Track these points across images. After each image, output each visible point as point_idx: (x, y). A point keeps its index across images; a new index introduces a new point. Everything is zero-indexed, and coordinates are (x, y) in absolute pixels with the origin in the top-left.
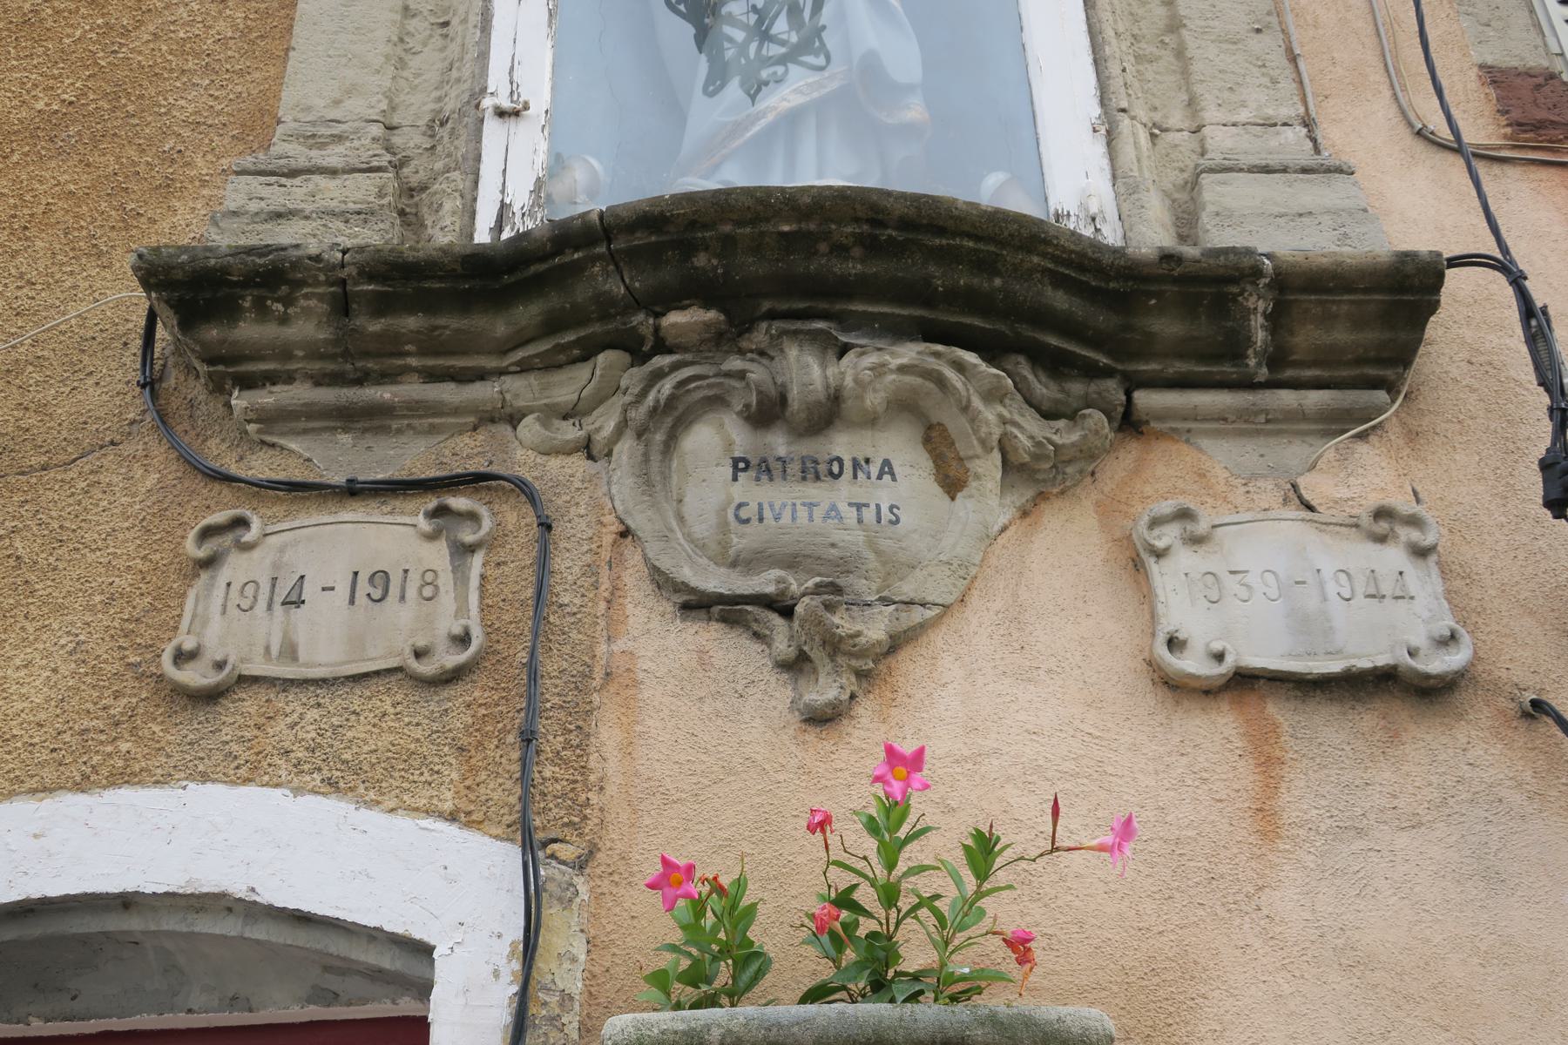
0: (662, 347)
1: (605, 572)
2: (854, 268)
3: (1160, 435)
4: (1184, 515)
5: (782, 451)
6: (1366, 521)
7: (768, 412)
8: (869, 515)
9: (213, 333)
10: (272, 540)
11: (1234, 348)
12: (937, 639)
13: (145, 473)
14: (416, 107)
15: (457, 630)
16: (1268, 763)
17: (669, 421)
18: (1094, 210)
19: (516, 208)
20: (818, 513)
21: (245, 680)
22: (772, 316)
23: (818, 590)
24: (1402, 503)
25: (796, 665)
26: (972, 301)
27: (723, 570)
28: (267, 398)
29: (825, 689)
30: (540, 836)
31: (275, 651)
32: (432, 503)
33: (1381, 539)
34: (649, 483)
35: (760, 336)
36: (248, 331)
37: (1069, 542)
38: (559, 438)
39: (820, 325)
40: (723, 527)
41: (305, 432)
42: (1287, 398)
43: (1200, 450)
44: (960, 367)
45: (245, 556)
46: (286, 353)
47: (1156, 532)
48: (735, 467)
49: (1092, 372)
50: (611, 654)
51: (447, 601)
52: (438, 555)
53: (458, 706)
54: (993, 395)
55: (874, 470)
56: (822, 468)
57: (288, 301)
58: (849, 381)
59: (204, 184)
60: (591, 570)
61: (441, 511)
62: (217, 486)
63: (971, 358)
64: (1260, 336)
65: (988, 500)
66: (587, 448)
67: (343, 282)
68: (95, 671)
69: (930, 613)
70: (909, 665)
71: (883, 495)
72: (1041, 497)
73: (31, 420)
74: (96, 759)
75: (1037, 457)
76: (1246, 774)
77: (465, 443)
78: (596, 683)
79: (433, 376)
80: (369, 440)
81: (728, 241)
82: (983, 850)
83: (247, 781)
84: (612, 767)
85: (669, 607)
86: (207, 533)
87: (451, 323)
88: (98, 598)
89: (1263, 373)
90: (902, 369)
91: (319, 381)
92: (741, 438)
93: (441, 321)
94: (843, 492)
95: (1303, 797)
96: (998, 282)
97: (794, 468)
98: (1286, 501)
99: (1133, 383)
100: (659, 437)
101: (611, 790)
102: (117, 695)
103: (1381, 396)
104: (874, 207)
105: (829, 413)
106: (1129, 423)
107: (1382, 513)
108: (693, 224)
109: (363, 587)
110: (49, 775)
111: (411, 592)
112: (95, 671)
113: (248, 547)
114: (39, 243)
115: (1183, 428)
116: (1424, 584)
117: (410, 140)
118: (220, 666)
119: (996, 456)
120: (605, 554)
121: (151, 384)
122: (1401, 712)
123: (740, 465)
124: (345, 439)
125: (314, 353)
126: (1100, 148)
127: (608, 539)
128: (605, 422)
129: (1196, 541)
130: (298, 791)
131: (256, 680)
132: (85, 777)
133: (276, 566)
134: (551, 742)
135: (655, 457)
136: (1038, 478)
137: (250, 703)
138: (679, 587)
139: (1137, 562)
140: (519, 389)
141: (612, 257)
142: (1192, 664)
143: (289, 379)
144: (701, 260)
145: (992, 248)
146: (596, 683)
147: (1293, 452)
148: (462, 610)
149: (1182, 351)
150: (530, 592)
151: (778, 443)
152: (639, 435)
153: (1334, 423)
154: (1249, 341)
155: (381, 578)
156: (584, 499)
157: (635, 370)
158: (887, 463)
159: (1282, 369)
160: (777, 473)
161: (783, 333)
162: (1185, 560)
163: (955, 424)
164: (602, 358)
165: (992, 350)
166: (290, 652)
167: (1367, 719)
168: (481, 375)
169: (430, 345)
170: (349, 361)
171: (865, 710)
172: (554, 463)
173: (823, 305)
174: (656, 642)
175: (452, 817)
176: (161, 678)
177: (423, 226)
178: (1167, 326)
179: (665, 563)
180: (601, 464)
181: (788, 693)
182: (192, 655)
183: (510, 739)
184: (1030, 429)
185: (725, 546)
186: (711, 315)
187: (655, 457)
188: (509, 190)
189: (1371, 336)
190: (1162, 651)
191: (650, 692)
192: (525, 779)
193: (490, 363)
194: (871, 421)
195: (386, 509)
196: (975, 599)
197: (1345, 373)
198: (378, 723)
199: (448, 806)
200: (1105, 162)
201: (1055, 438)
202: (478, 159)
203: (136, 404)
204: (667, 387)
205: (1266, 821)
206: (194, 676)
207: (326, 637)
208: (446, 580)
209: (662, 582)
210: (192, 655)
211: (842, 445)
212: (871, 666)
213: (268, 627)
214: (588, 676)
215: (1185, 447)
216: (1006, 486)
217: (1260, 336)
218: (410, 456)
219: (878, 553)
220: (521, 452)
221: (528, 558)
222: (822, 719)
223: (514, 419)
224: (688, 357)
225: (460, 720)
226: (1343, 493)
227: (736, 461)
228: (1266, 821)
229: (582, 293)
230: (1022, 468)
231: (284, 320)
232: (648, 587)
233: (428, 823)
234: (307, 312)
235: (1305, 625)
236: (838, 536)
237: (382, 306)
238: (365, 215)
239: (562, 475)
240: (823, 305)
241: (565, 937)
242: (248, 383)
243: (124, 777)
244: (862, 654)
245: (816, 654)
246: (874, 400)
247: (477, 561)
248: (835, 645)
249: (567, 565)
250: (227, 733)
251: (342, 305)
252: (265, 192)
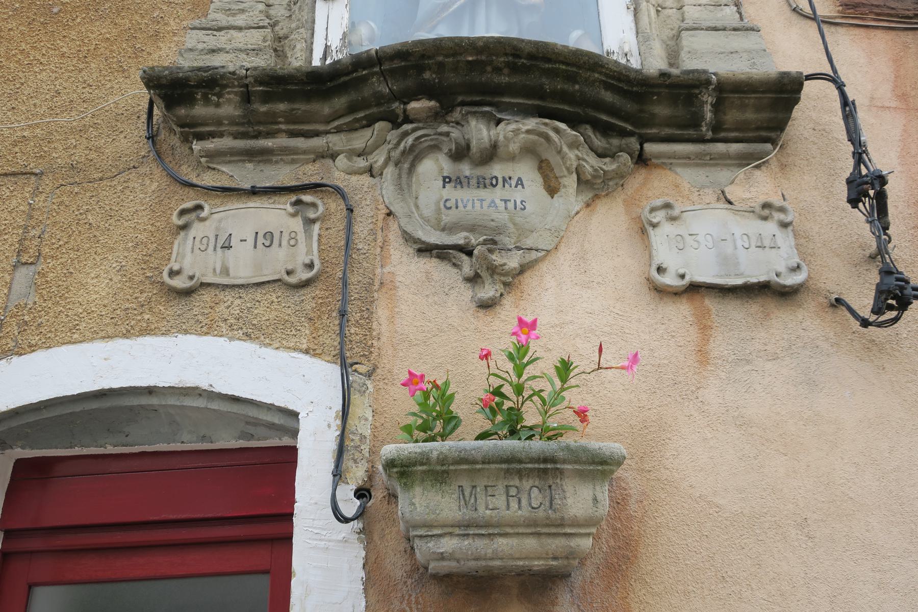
0: (407, 120)
1: (379, 233)
2: (504, 79)
3: (657, 166)
4: (667, 206)
5: (467, 173)
6: (758, 209)
7: (460, 153)
8: (511, 205)
9: (182, 111)
10: (215, 216)
11: (695, 122)
12: (544, 267)
13: (150, 184)
15: (307, 261)
16: (705, 329)
17: (411, 157)
18: (626, 50)
19: (333, 48)
20: (485, 204)
21: (204, 285)
22: (463, 104)
23: (485, 243)
24: (777, 201)
25: (474, 280)
26: (563, 97)
27: (438, 232)
28: (211, 145)
29: (488, 291)
30: (349, 361)
31: (218, 271)
32: (294, 198)
33: (765, 218)
34: (401, 189)
35: (457, 115)
36: (200, 110)
37: (608, 221)
39: (487, 109)
40: (438, 211)
41: (230, 162)
42: (721, 147)
43: (676, 173)
44: (557, 131)
45: (202, 224)
46: (219, 122)
47: (653, 214)
48: (444, 181)
49: (623, 133)
50: (383, 273)
51: (302, 247)
52: (297, 224)
53: (308, 299)
54: (573, 145)
55: (513, 183)
56: (488, 182)
57: (220, 95)
58: (501, 138)
59: (175, 34)
60: (373, 232)
61: (298, 202)
62: (187, 189)
63: (563, 126)
64: (709, 115)
65: (570, 197)
66: (370, 171)
67: (247, 86)
68: (130, 280)
69: (540, 254)
70: (529, 280)
71: (518, 195)
72: (597, 196)
73: (93, 155)
74: (133, 323)
75: (594, 177)
76: (693, 334)
77: (310, 168)
78: (376, 287)
79: (293, 134)
80: (262, 166)
81: (441, 65)
82: (564, 368)
83: (207, 334)
84: (384, 328)
85: (411, 251)
86: (183, 212)
87: (301, 107)
88: (130, 244)
89: (710, 135)
90: (528, 132)
91: (236, 136)
92: (447, 166)
93: (296, 106)
94: (498, 194)
95: (719, 346)
96: (577, 87)
97: (474, 182)
98: (718, 199)
99: (643, 139)
100: (406, 166)
101: (384, 339)
102: (142, 292)
103: (769, 146)
104: (515, 48)
105: (491, 154)
106: (641, 160)
107: (766, 206)
108: (423, 56)
109: (261, 240)
110: (110, 330)
111: (284, 243)
112: (130, 280)
113: (203, 220)
114: (93, 65)
115: (668, 163)
116: (785, 241)
118: (191, 278)
119: (575, 176)
120: (380, 224)
121: (152, 138)
122: (771, 304)
123: (446, 180)
124: (250, 166)
125: (233, 122)
126: (630, 18)
127: (381, 217)
128: (379, 158)
129: (673, 219)
130: (231, 339)
131: (209, 285)
132: (128, 331)
133: (217, 229)
134: (354, 316)
135: (404, 176)
136: (594, 187)
137: (207, 296)
138: (416, 241)
140: (336, 141)
141: (382, 73)
142: (669, 280)
143: (221, 135)
144: (427, 75)
145: (574, 69)
146: (376, 287)
147: (722, 175)
148: (309, 251)
149: (670, 122)
150: (343, 243)
151: (466, 169)
152: (396, 165)
153: (744, 160)
154: (703, 118)
155: (269, 235)
156: (369, 197)
157: (394, 131)
158: (520, 179)
159: (719, 133)
160: (465, 184)
161: (468, 113)
162: (667, 228)
163: (554, 159)
164: (378, 126)
165: (573, 122)
166: (226, 271)
167: (754, 307)
168: (317, 134)
169: (291, 118)
170: (252, 126)
171: (507, 301)
172: (354, 179)
173: (488, 99)
174: (405, 268)
175: (307, 352)
176: (163, 283)
177: (286, 57)
178: (662, 110)
179: (409, 229)
180: (378, 179)
181: (469, 293)
182: (178, 273)
183: (334, 314)
184: (592, 162)
185: (439, 220)
186: (432, 103)
187: (404, 176)
188: (330, 38)
189: (765, 115)
190: (654, 273)
192: (342, 334)
193: (321, 128)
194: (512, 158)
195: (271, 201)
196: (562, 248)
197: (751, 134)
198: (269, 307)
199: (304, 346)
200: (633, 25)
201: (604, 167)
202: (313, 22)
203: (145, 148)
204: (410, 140)
205: (703, 356)
206: (179, 283)
207: (243, 264)
208: (301, 237)
209: (408, 238)
210: (178, 273)
211: (497, 170)
212: (511, 280)
213: (215, 259)
214: (371, 284)
215: (668, 172)
216: (579, 191)
217: (709, 115)
219: (514, 224)
220: (337, 173)
221: (342, 226)
222: (486, 306)
223: (333, 156)
224: (421, 125)
225: (309, 305)
226: (747, 195)
227: (444, 178)
228: (703, 356)
229: (367, 92)
230: (587, 182)
231: (218, 105)
232: (401, 241)
233: (295, 354)
234: (229, 101)
235: (727, 261)
236: (495, 216)
237: (267, 98)
238: (257, 51)
240: (488, 99)
241: (361, 408)
242: (200, 137)
243: (146, 331)
244: (506, 274)
245: (484, 274)
246: (514, 147)
247: (316, 227)
248: (493, 270)
249: (361, 229)
250: (196, 311)
251: (247, 98)
252: (206, 39)
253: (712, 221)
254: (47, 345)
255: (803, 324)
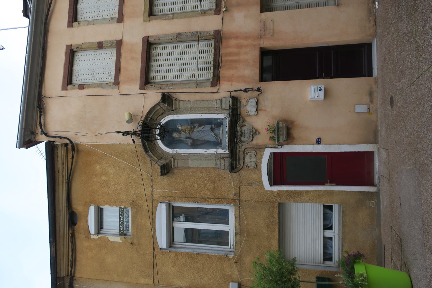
0: (237, 141)
7: (241, 136)
11: (236, 108)
13: (242, 172)
14: (215, 159)
16: (261, 110)
25: (256, 134)
29: (257, 133)
36: (234, 166)
37: (247, 119)
38: (241, 148)
52: (249, 154)
54: (240, 123)
65: (245, 123)
71: (246, 129)
82: (269, 126)
94: (246, 132)
95: (263, 108)
105: (241, 132)
106: (240, 115)
115: (240, 112)
116: (251, 100)
117: (217, 159)
121: (235, 172)
128: (240, 145)
136: (244, 121)
137: (257, 163)
139: (249, 115)
140: (238, 150)
142: (256, 113)
147: (242, 105)
151: (243, 135)
153: (240, 102)
159: (237, 106)
162: (250, 113)
165: (237, 123)
167: (259, 104)
170: (236, 160)
174: (254, 142)
178: (235, 112)
184: (241, 121)
191: (257, 142)
198: (258, 156)
205: (264, 110)
206: (255, 166)
207: (253, 160)
209: (251, 142)
211: (243, 132)
212: (256, 131)
213: (253, 163)
218: (242, 156)
220: (242, 150)
222: (259, 133)
228: (264, 110)
235: (254, 107)
238: (225, 161)
239: (243, 147)
241: (270, 146)
243: (261, 169)
248: (255, 132)
253: (248, 107)
254: (262, 180)
255: (261, 98)
